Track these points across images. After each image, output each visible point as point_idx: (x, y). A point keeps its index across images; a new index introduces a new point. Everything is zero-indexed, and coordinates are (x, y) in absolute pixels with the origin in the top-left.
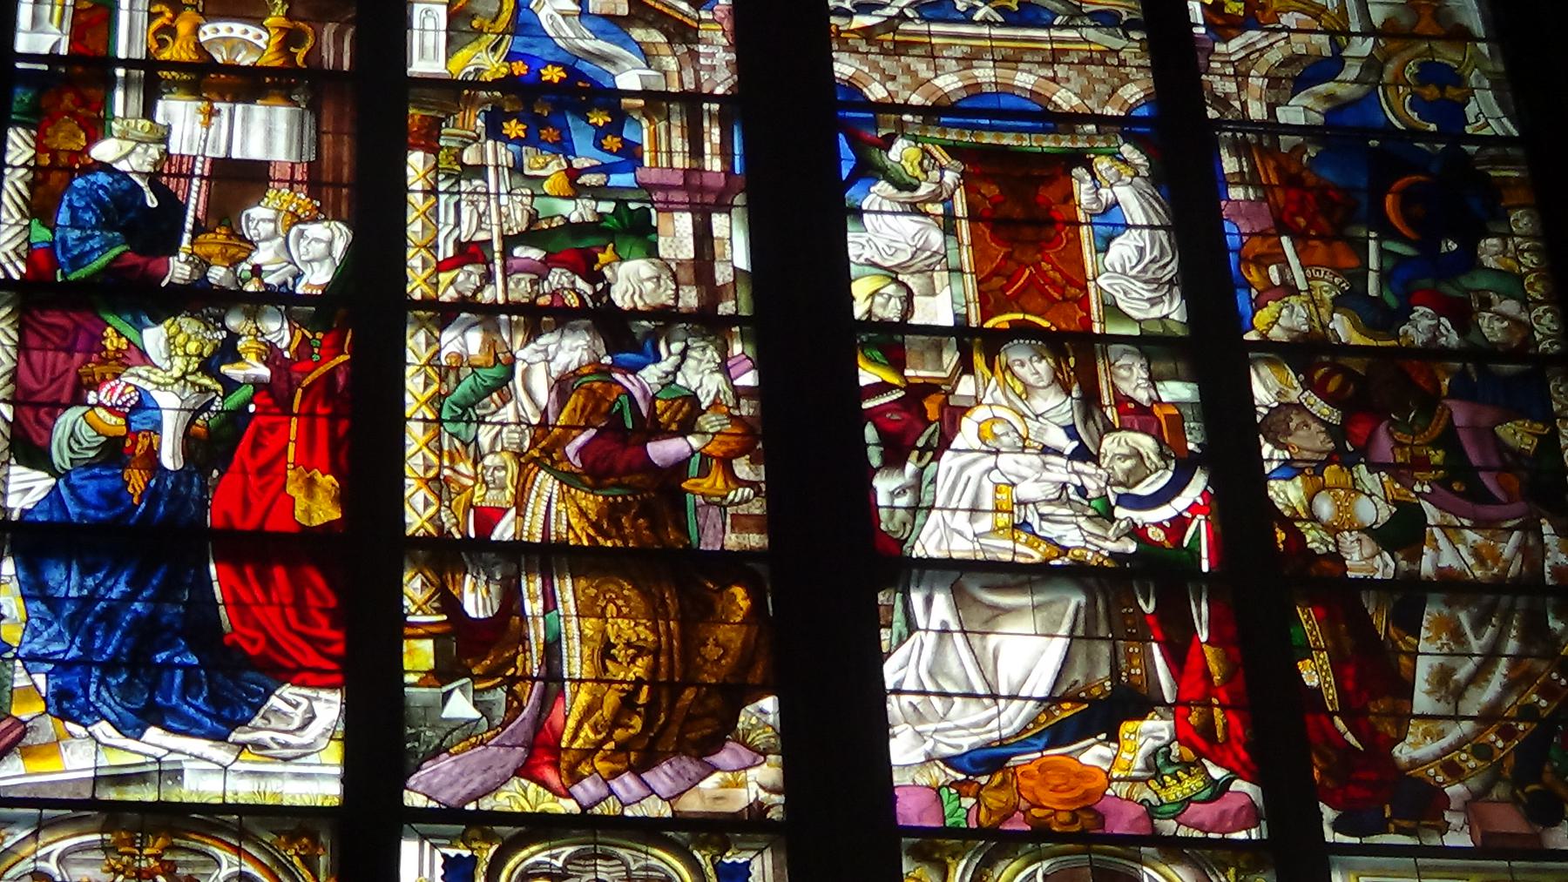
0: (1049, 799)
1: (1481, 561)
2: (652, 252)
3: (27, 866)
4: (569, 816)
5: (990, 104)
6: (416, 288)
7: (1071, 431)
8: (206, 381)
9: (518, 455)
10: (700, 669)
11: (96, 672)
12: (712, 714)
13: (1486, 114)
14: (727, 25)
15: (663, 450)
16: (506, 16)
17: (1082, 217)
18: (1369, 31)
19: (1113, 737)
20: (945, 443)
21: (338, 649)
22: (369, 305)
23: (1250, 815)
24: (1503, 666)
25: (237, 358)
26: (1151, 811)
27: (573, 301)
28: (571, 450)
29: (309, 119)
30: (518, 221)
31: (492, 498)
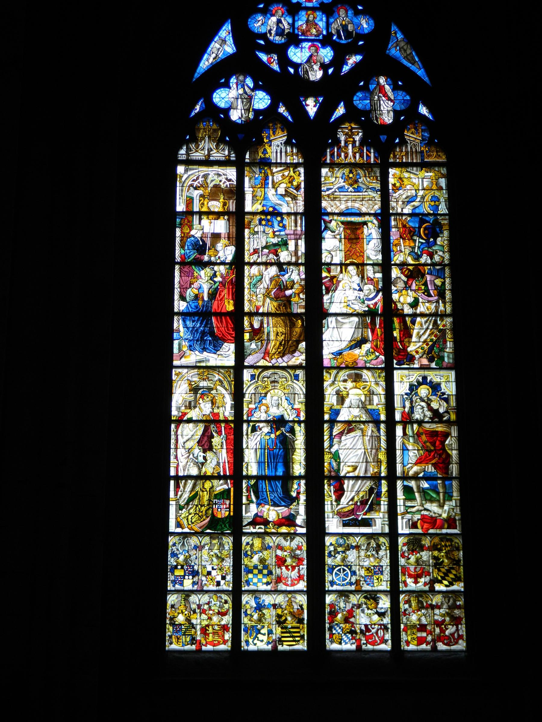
0: (349, 360)
1: (428, 310)
2: (287, 249)
3: (186, 378)
6: (247, 260)
7: (359, 286)
8: (211, 282)
9: (263, 295)
12: (294, 346)
13: (443, 209)
14: (303, 195)
15: (288, 292)
16: (263, 196)
17: (365, 237)
18: (424, 189)
19: (360, 348)
21: (234, 335)
22: (238, 263)
23: (382, 362)
24: (429, 330)
25: (216, 277)
26: (366, 362)
27: (273, 261)
28: (272, 293)
29: (228, 223)
30: (264, 244)
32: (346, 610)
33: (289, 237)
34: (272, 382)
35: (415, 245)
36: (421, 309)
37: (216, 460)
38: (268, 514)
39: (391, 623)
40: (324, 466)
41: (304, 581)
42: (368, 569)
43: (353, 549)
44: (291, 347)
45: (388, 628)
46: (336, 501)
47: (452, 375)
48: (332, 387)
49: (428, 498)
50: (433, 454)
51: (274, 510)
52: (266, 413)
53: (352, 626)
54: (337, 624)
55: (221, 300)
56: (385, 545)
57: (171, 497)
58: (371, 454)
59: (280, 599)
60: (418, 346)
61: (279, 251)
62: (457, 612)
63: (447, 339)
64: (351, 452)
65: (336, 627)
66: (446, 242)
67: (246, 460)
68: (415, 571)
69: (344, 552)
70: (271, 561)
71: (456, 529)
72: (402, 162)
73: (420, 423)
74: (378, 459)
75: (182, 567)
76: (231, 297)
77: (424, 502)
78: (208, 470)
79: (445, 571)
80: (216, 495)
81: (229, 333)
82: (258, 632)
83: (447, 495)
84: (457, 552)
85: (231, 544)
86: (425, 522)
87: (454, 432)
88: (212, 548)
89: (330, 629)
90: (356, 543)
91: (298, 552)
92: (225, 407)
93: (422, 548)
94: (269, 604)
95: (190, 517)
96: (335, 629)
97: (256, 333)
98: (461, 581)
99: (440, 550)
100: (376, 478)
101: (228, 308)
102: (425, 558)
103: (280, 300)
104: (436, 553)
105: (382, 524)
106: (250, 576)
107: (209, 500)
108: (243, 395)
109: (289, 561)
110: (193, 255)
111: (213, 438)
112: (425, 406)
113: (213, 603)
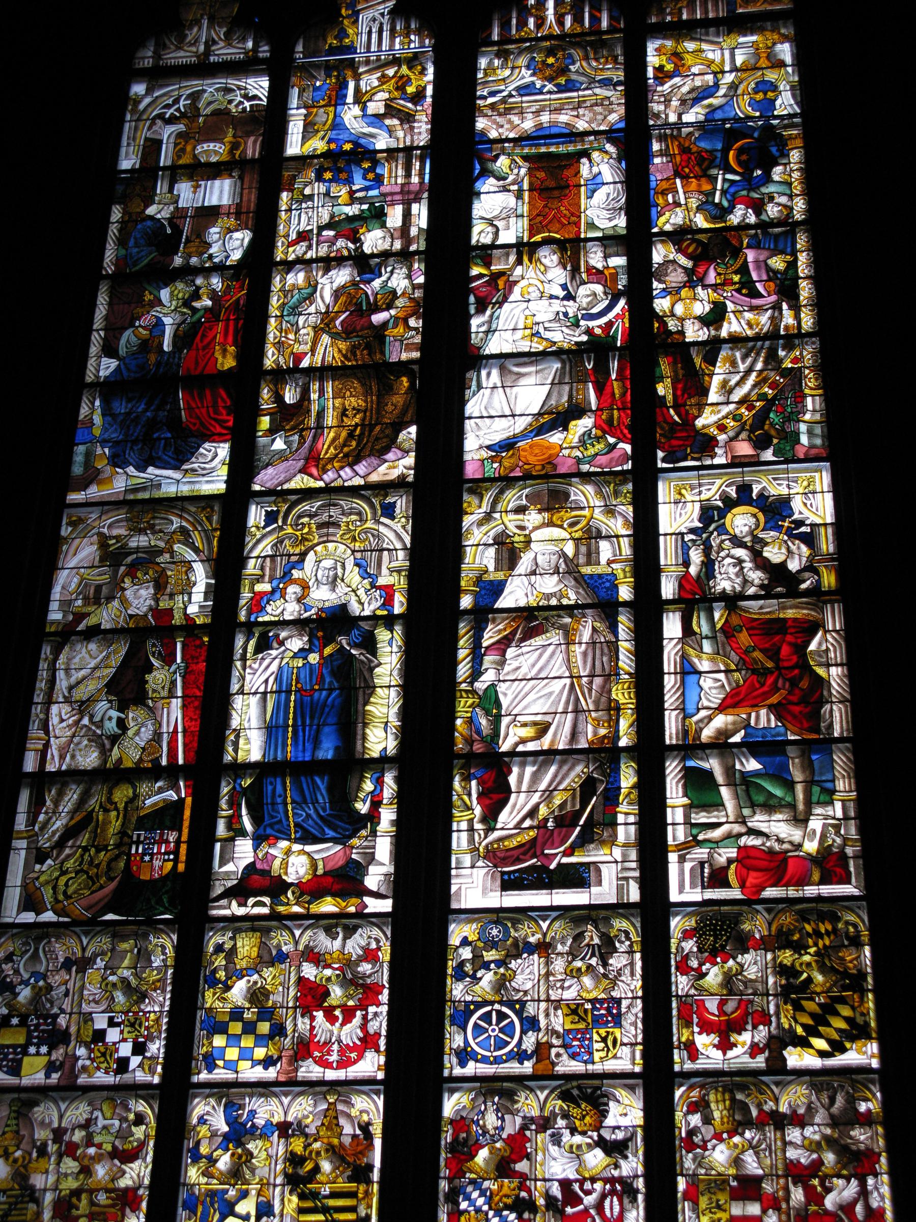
0: (532, 459)
2: (383, 225)
4: (320, 488)
5: (547, 133)
6: (279, 256)
7: (564, 287)
9: (314, 328)
10: (384, 417)
11: (129, 445)
12: (387, 436)
13: (786, 103)
14: (429, 112)
15: (378, 318)
16: (330, 122)
17: (582, 182)
18: (735, 69)
19: (566, 429)
20: (505, 299)
21: (231, 424)
23: (625, 458)
24: (754, 374)
26: (579, 461)
27: (345, 253)
28: (338, 322)
29: (239, 184)
30: (326, 218)
31: (298, 349)
32: (504, 1136)
33: (389, 198)
34: (320, 526)
35: (715, 189)
36: (732, 326)
37: (150, 727)
38: (285, 864)
39: (646, 1176)
40: (453, 728)
41: (378, 1051)
42: (574, 1012)
43: (531, 953)
44: (377, 439)
45: (637, 1191)
46: (483, 820)
47: (823, 479)
48: (484, 529)
49: (760, 799)
50: (770, 680)
51: (303, 852)
52: (299, 601)
53: (522, 1187)
54: (473, 1182)
55: (204, 348)
56: (628, 938)
57: (17, 828)
58: (590, 690)
59: (302, 1108)
60: (723, 413)
61: (361, 231)
62: (860, 1135)
63: (807, 391)
64: (532, 690)
65: (469, 1189)
66: (796, 175)
67: (235, 723)
68: (722, 1012)
69: (500, 963)
70: (283, 995)
71: (849, 883)
72: (680, 20)
73: (731, 600)
74: (610, 700)
75: (23, 1023)
76: (230, 339)
77: (746, 812)
78: (130, 752)
79: (817, 1010)
80: (141, 819)
81: (216, 420)
82: (226, 1211)
83: (816, 790)
84: (853, 949)
85: (170, 951)
86: (749, 869)
87: (834, 619)
88: (115, 963)
89: (453, 1197)
90: (539, 936)
91: (366, 968)
92: (190, 594)
93: (743, 943)
94: (268, 1123)
95: (63, 880)
96: (468, 1198)
97: (288, 417)
98: (869, 1038)
99: (799, 948)
100: (606, 754)
101: (222, 364)
102: (752, 972)
103: (357, 336)
104: (787, 957)
105: (618, 879)
106: (219, 1041)
107: (123, 833)
108: (242, 561)
109: (337, 993)
110: (148, 257)
111: (150, 672)
112: (747, 559)
113: (101, 1122)
